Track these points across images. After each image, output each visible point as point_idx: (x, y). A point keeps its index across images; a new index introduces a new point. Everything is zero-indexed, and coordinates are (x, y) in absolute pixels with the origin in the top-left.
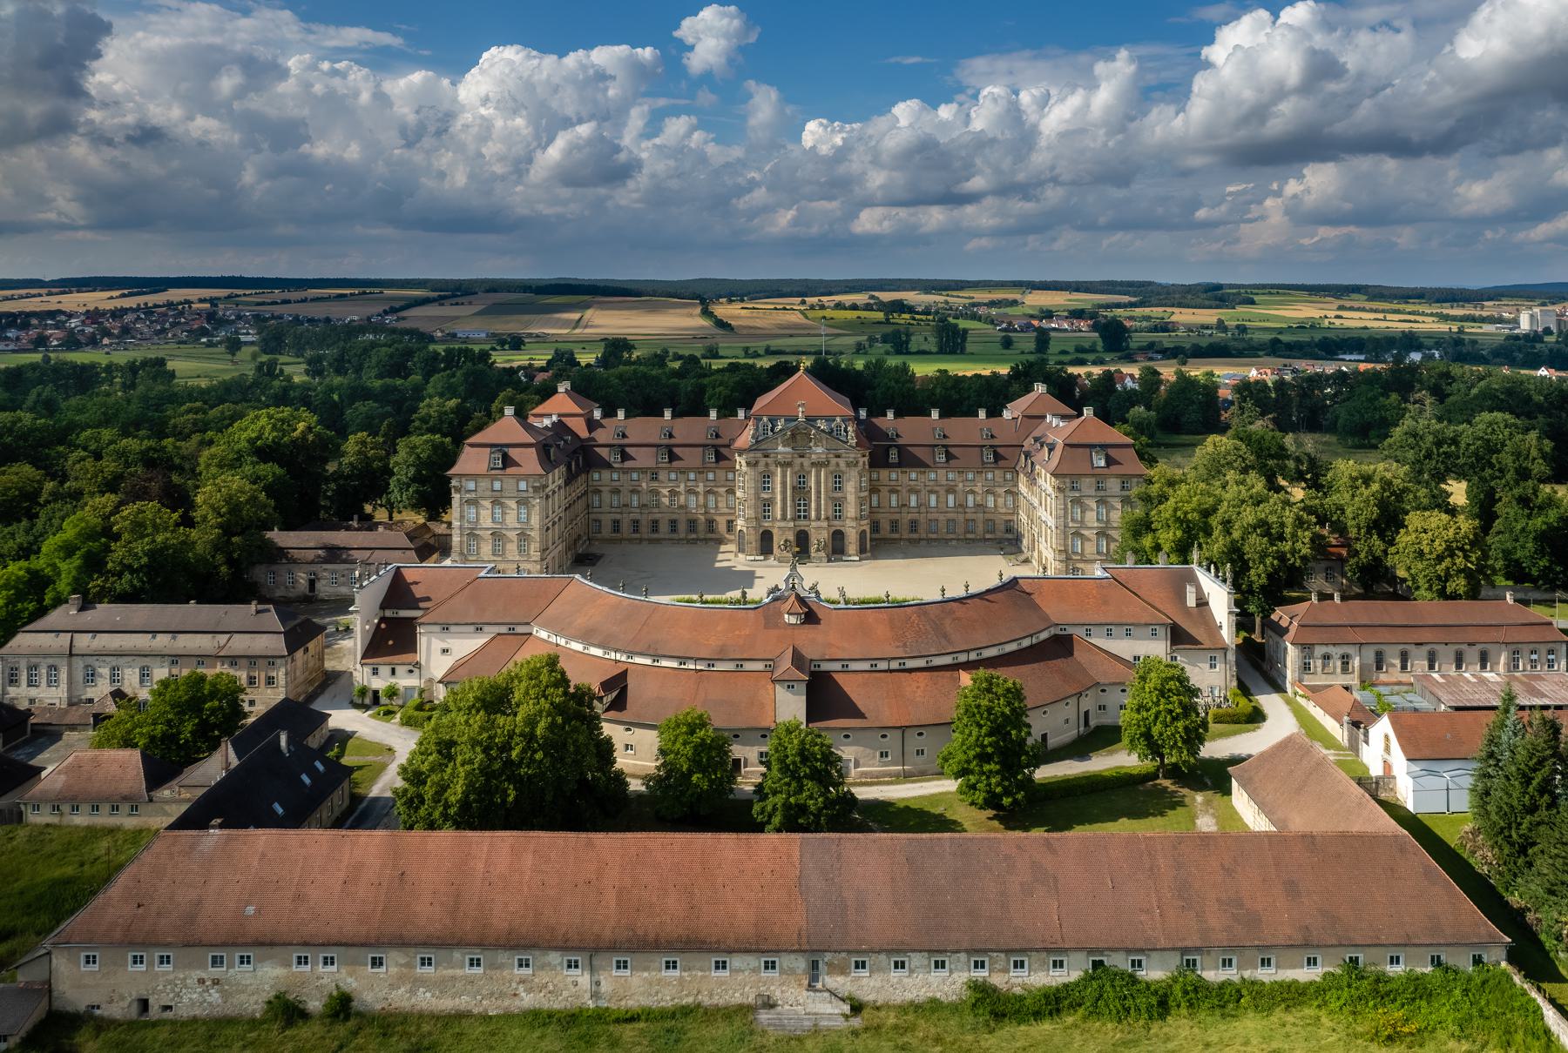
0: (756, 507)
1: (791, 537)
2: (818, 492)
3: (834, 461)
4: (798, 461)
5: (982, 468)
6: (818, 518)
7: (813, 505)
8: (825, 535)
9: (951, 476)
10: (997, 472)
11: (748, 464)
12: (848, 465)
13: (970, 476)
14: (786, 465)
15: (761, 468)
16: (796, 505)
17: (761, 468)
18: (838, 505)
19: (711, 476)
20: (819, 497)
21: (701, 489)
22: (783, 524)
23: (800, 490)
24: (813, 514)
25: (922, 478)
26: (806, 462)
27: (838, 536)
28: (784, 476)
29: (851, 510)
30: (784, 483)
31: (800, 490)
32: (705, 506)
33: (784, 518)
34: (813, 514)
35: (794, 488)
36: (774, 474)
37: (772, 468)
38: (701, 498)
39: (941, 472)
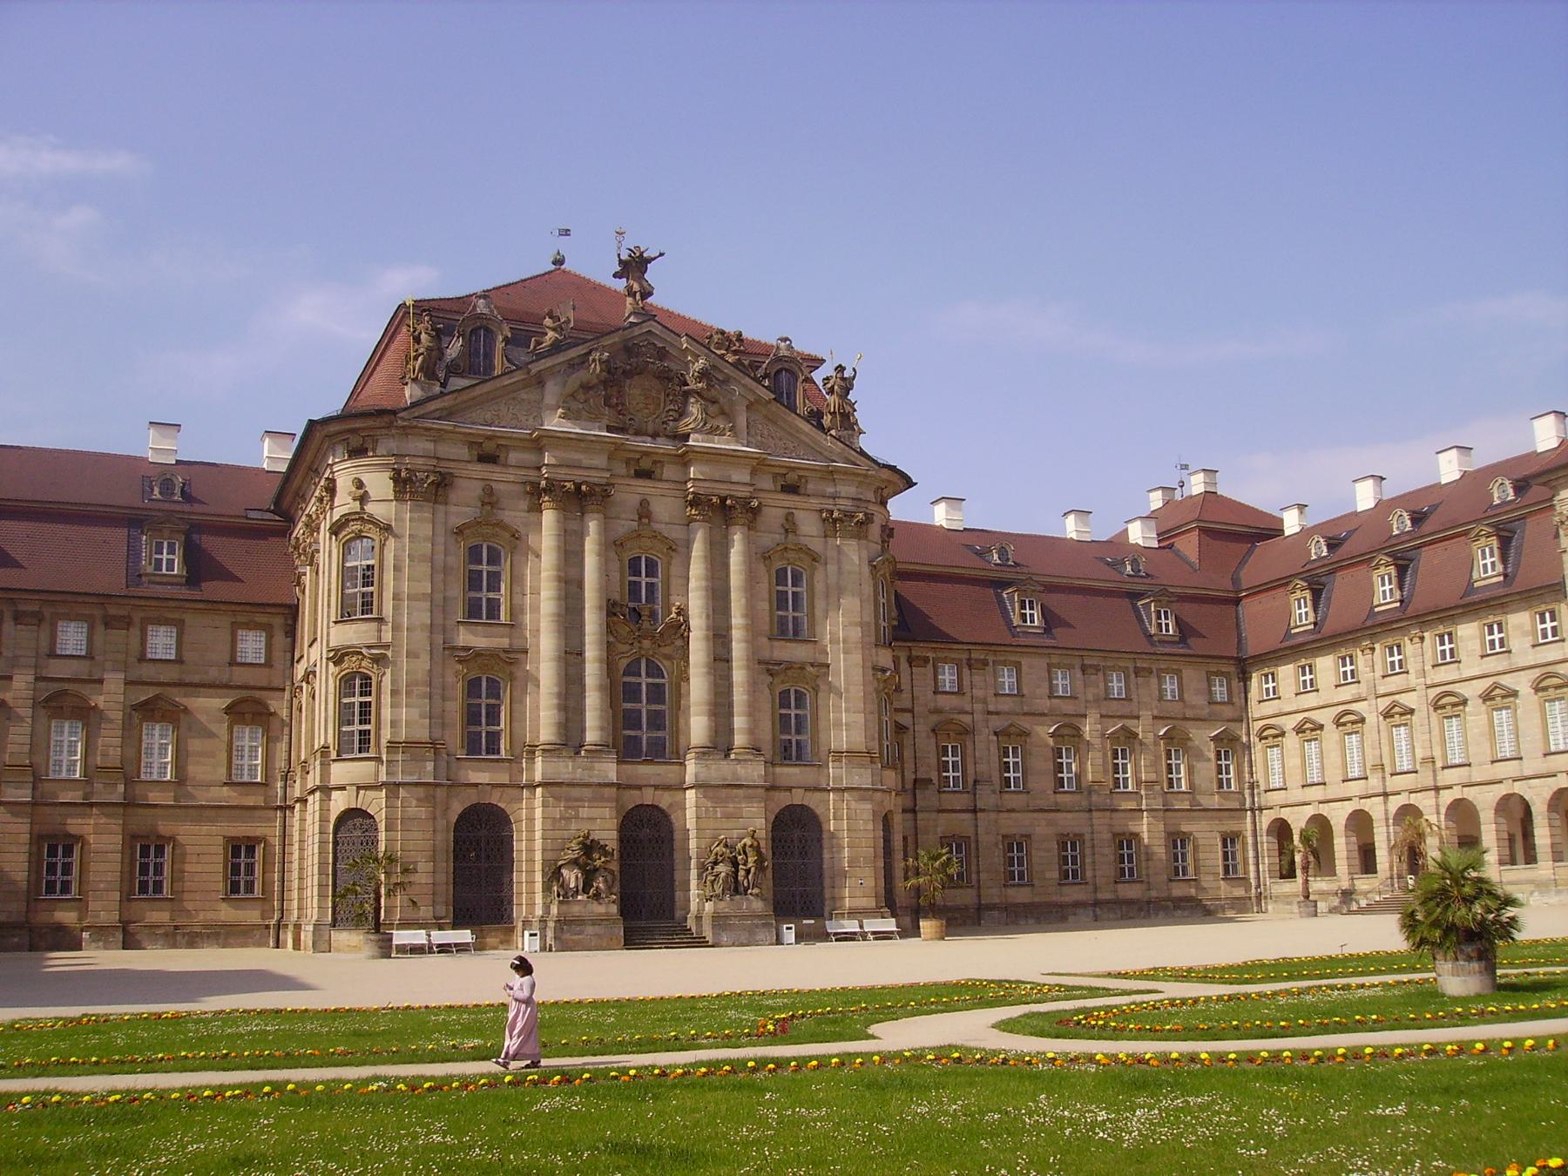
0: (434, 690)
1: (607, 833)
2: (719, 637)
3: (775, 507)
4: (630, 493)
5: (1146, 659)
6: (720, 744)
7: (698, 687)
8: (754, 821)
9: (1061, 682)
10: (1189, 673)
11: (403, 484)
12: (832, 523)
13: (1117, 685)
14: (578, 499)
15: (463, 506)
16: (620, 691)
17: (463, 506)
18: (792, 695)
19: (162, 642)
20: (720, 659)
21: (110, 696)
22: (566, 769)
23: (640, 619)
24: (698, 727)
25: (979, 683)
26: (666, 508)
27: (796, 834)
28: (570, 555)
29: (845, 720)
30: (570, 587)
31: (640, 619)
32: (128, 771)
33: (570, 740)
34: (698, 727)
35: (611, 609)
36: (517, 540)
37: (514, 514)
38: (110, 743)
39: (1034, 667)
